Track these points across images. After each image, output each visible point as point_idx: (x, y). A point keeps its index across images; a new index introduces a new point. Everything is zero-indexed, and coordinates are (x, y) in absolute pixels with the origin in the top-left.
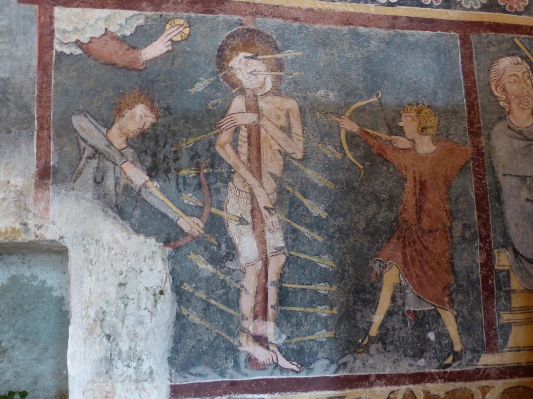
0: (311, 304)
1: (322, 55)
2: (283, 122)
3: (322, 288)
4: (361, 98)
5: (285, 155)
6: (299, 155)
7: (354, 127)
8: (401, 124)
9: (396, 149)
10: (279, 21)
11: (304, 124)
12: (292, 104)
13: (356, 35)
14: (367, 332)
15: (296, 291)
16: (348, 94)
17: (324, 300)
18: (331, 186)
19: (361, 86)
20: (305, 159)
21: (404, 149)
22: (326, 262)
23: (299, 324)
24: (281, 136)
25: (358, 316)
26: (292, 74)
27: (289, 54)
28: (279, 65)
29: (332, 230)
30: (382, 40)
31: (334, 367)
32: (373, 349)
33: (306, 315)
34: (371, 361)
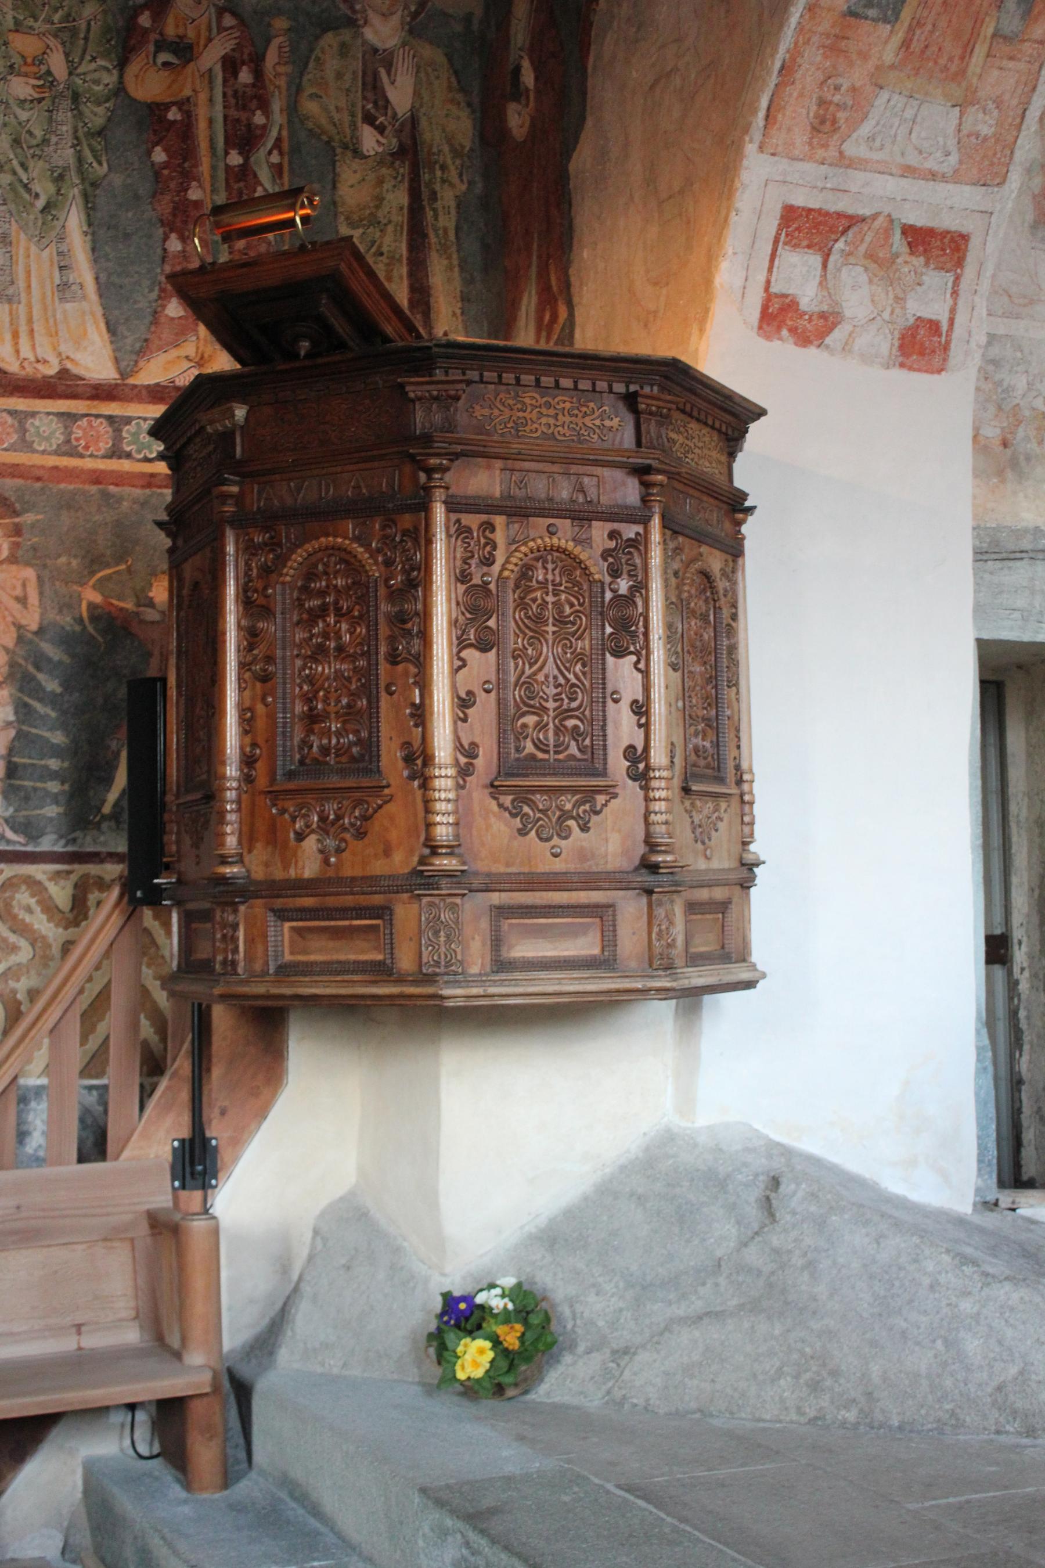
0: (42, 778)
1: (66, 519)
2: (18, 592)
3: (54, 764)
4: (108, 565)
5: (19, 627)
6: (34, 627)
7: (97, 598)
8: (151, 594)
9: (142, 622)
10: (19, 482)
11: (41, 593)
12: (30, 573)
13: (106, 495)
14: (99, 810)
15: (25, 766)
16: (92, 561)
17: (54, 775)
18: (67, 660)
19: (108, 552)
20: (41, 631)
21: (153, 623)
22: (58, 738)
23: (27, 798)
24: (16, 607)
25: (91, 793)
26: (31, 539)
27: (29, 518)
28: (17, 530)
29: (66, 705)
30: (135, 501)
31: (63, 842)
32: (105, 826)
33: (35, 789)
34: (102, 839)
